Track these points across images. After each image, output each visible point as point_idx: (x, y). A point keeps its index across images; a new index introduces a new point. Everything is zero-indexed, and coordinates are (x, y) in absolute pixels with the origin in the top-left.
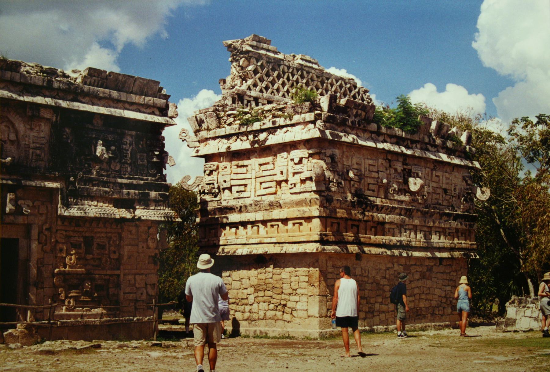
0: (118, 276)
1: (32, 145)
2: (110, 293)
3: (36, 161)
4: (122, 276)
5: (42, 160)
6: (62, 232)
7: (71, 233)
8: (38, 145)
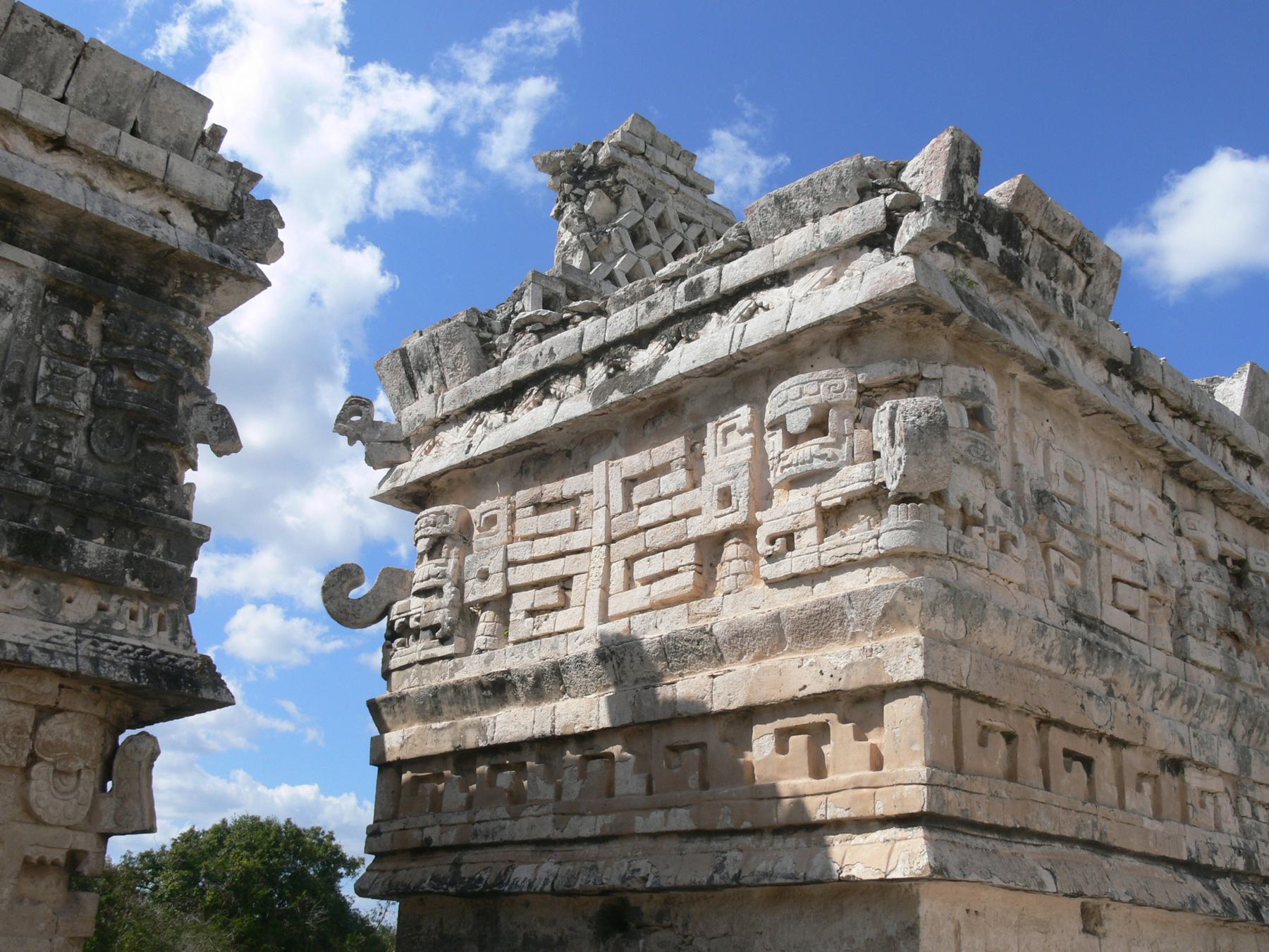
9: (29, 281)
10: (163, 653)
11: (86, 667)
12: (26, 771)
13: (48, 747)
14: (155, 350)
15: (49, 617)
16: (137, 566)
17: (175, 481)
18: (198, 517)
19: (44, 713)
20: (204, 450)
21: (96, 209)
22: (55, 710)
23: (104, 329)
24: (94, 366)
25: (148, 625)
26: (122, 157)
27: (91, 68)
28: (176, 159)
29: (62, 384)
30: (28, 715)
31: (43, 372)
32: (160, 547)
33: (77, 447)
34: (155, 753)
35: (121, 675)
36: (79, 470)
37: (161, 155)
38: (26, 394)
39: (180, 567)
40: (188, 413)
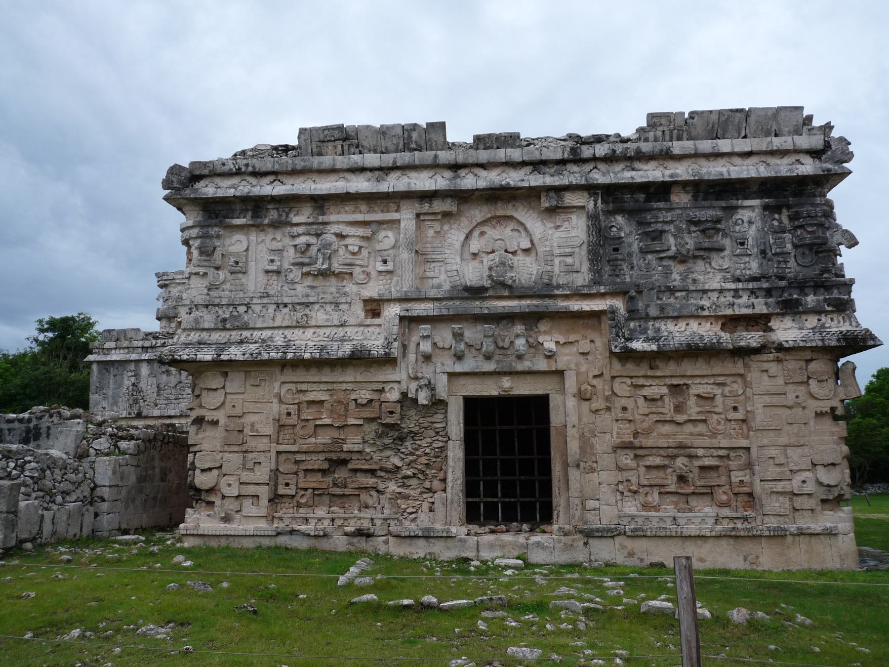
0: (748, 449)
1: (557, 251)
2: (735, 480)
4: (754, 451)
6: (625, 380)
7: (641, 381)
8: (568, 250)
9: (757, 210)
10: (848, 331)
11: (820, 344)
12: (807, 383)
13: (813, 373)
14: (812, 217)
15: (801, 329)
17: (834, 264)
18: (848, 276)
19: (808, 361)
20: (842, 248)
21: (773, 174)
22: (811, 360)
23: (789, 216)
24: (789, 232)
25: (839, 322)
26: (775, 148)
27: (752, 119)
29: (782, 244)
30: (803, 364)
31: (772, 241)
32: (836, 291)
33: (792, 263)
34: (855, 368)
35: (834, 343)
37: (790, 139)
38: (768, 251)
39: (846, 297)
40: (832, 237)
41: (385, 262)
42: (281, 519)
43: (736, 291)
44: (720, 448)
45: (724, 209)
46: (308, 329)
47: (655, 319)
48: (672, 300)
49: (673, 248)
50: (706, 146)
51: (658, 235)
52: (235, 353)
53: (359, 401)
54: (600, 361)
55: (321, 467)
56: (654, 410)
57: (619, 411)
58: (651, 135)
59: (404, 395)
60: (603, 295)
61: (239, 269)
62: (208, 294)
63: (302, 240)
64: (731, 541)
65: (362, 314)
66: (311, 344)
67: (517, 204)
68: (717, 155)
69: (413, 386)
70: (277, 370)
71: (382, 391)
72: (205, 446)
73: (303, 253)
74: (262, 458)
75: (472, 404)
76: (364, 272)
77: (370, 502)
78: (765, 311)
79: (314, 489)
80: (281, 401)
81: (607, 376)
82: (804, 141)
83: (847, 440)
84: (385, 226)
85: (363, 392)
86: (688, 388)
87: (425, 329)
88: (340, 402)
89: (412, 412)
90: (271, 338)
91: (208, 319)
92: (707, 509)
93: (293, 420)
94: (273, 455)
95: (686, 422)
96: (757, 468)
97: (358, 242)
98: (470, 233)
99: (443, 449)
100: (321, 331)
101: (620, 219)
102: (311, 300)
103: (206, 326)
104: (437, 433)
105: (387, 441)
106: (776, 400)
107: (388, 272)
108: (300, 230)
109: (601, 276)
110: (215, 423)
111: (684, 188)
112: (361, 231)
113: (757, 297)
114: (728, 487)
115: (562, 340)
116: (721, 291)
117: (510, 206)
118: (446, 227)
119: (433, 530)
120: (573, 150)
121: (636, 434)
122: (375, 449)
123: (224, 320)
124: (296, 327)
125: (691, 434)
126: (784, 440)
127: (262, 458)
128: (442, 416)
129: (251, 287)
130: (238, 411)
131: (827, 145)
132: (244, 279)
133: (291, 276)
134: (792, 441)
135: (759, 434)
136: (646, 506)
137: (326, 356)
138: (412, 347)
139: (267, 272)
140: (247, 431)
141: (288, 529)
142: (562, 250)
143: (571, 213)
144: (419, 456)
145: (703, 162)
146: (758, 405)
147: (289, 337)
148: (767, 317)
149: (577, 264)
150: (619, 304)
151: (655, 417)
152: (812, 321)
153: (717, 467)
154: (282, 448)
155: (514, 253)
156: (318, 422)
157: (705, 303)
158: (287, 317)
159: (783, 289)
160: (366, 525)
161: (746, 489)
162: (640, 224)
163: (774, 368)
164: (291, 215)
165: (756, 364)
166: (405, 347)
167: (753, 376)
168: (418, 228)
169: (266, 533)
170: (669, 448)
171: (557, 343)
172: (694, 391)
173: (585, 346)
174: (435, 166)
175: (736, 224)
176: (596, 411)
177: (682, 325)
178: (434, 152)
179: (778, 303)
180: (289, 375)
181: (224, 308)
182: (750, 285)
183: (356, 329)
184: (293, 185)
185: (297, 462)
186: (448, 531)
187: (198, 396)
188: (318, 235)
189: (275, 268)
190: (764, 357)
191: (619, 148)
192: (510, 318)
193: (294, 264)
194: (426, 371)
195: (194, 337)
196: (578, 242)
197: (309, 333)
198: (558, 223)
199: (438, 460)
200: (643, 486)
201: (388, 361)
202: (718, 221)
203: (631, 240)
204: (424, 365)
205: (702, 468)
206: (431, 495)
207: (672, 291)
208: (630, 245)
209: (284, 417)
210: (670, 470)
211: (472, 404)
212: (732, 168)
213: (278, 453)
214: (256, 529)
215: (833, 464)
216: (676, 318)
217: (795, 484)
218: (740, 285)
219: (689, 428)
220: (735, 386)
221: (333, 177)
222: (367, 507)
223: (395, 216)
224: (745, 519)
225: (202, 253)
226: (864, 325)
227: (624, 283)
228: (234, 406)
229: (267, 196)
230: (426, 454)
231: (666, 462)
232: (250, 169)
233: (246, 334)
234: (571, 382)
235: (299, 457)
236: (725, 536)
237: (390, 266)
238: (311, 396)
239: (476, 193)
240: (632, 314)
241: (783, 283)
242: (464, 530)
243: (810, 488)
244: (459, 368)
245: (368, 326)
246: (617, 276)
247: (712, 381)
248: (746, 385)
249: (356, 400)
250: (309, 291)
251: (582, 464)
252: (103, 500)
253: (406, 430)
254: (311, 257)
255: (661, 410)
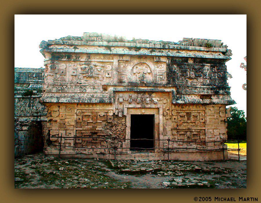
0: (205, 130)
1: (158, 74)
2: (201, 138)
3: (161, 80)
4: (206, 130)
5: (163, 80)
7: (179, 111)
8: (161, 74)
11: (223, 103)
13: (221, 111)
16: (226, 92)
18: (229, 86)
19: (220, 108)
20: (229, 78)
21: (214, 57)
24: (217, 73)
28: (219, 48)
29: (215, 77)
33: (217, 81)
36: (218, 84)
41: (108, 74)
42: (77, 150)
43: (204, 88)
44: (198, 129)
45: (201, 66)
46: (85, 94)
47: (183, 94)
48: (188, 90)
49: (189, 75)
50: (198, 48)
51: (186, 71)
52: (63, 100)
53: (101, 115)
54: (168, 106)
55: (89, 135)
56: (182, 119)
57: (173, 119)
58: (184, 44)
59: (114, 114)
60: (170, 87)
61: (63, 73)
62: (54, 82)
63: (83, 66)
64: (200, 153)
65: (102, 90)
66: (86, 98)
67: (147, 60)
68: (200, 51)
69: (117, 111)
70: (76, 105)
71: (107, 113)
72: (53, 128)
73: (83, 70)
74: (71, 132)
75: (133, 117)
76: (102, 77)
77: (104, 144)
78: (211, 94)
79: (87, 141)
80: (77, 115)
81: (171, 110)
82: (222, 50)
83: (227, 128)
84: (108, 63)
85: (102, 113)
86: (191, 113)
87: (121, 95)
88: (95, 116)
89: (116, 119)
90: (74, 96)
91: (54, 90)
92: (194, 145)
93: (81, 121)
94: (75, 131)
95: (190, 122)
96: (207, 135)
97: (100, 67)
98: (133, 67)
99: (125, 129)
100: (90, 94)
101: (175, 66)
102: (86, 85)
103: (54, 92)
104: (123, 125)
105: (108, 127)
106: (212, 117)
107: (109, 77)
108: (83, 63)
109: (170, 82)
110: (56, 121)
111: (192, 59)
112: (101, 65)
113: (209, 90)
114: (199, 140)
115: (159, 99)
116: (200, 88)
117: (145, 60)
118: (126, 65)
119: (123, 152)
120: (163, 46)
121: (177, 126)
122: (104, 129)
123: (59, 90)
124: (82, 93)
125: (191, 126)
126: (213, 128)
127: (71, 132)
128: (124, 120)
129: (67, 80)
130: (64, 118)
131: (227, 51)
132: (65, 77)
133: (80, 77)
134: (215, 128)
135: (208, 126)
136: (179, 145)
137: (92, 102)
138: (116, 100)
139: (72, 75)
140: (67, 124)
141: (80, 152)
142: (159, 74)
143: (162, 63)
144: (117, 132)
145: (196, 52)
146: (208, 119)
147: (80, 96)
148: (211, 95)
149: (163, 78)
150: (174, 90)
151: (182, 121)
152: (221, 97)
153: (197, 134)
154: (77, 129)
155: (146, 74)
156: (88, 121)
157: (197, 91)
158: (79, 90)
159: (214, 88)
160: (103, 151)
161: (204, 140)
162: (180, 68)
163: (212, 109)
164: (80, 59)
165: (208, 108)
166: (114, 100)
167: (207, 111)
168: (119, 64)
169: (73, 154)
170: (186, 129)
171: (158, 100)
172: (192, 114)
173: (165, 101)
174: (124, 47)
175: (204, 70)
176: (167, 120)
177: (190, 97)
178: (124, 43)
179: (214, 92)
180: (80, 107)
181: (59, 86)
182: (207, 87)
183: (101, 94)
184: (81, 49)
185: (82, 133)
186: (127, 152)
187: (50, 113)
188: (88, 65)
189: (74, 74)
190: (210, 106)
191: (176, 46)
192: (144, 92)
193: (81, 74)
194: (121, 107)
195: (50, 95)
196: (164, 72)
197: (86, 94)
198: (158, 66)
199: (123, 132)
200: (179, 140)
201: (110, 104)
202: (200, 69)
203: (178, 72)
204: (120, 105)
205: (194, 135)
206: (120, 142)
207: (188, 87)
208: (178, 74)
209: (78, 120)
210: (185, 135)
211: (133, 117)
212: (204, 55)
213: (76, 130)
214: (70, 152)
215: (224, 134)
216: (189, 95)
217: (215, 139)
218: (205, 87)
219: (191, 124)
220: (202, 113)
221: (93, 48)
222: (103, 146)
223: (112, 61)
224: (203, 148)
225: (51, 69)
226: (233, 99)
227: (176, 84)
228: (62, 116)
229: (73, 52)
230: (119, 131)
231: (185, 133)
232: (68, 44)
233: (66, 94)
234: (161, 111)
235: (83, 132)
236: (198, 152)
237: (110, 76)
238: (86, 114)
239: (136, 56)
240: (178, 93)
241: (215, 87)
242: (130, 152)
243: (219, 140)
244: (130, 106)
245: (103, 93)
246: (174, 82)
247: (197, 112)
248: (205, 113)
249: (100, 115)
250: (85, 82)
251: (163, 134)
252: (22, 145)
253: (113, 124)
254: (86, 72)
255: (184, 119)
